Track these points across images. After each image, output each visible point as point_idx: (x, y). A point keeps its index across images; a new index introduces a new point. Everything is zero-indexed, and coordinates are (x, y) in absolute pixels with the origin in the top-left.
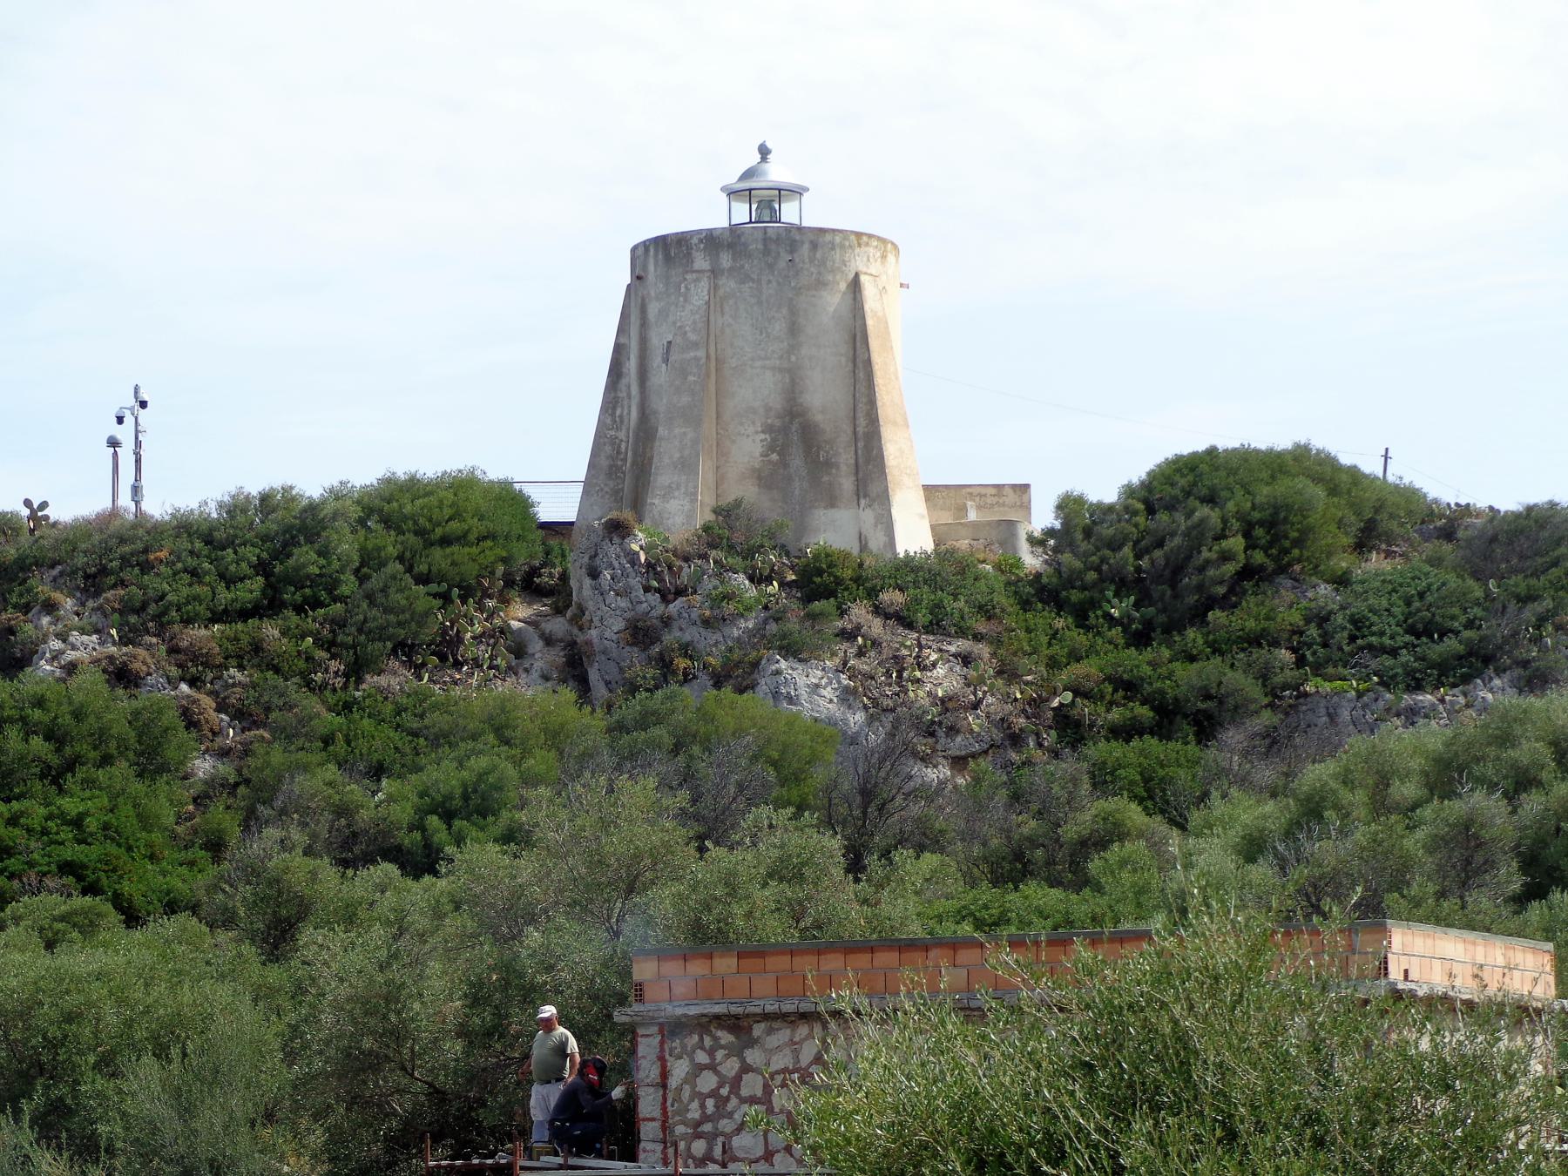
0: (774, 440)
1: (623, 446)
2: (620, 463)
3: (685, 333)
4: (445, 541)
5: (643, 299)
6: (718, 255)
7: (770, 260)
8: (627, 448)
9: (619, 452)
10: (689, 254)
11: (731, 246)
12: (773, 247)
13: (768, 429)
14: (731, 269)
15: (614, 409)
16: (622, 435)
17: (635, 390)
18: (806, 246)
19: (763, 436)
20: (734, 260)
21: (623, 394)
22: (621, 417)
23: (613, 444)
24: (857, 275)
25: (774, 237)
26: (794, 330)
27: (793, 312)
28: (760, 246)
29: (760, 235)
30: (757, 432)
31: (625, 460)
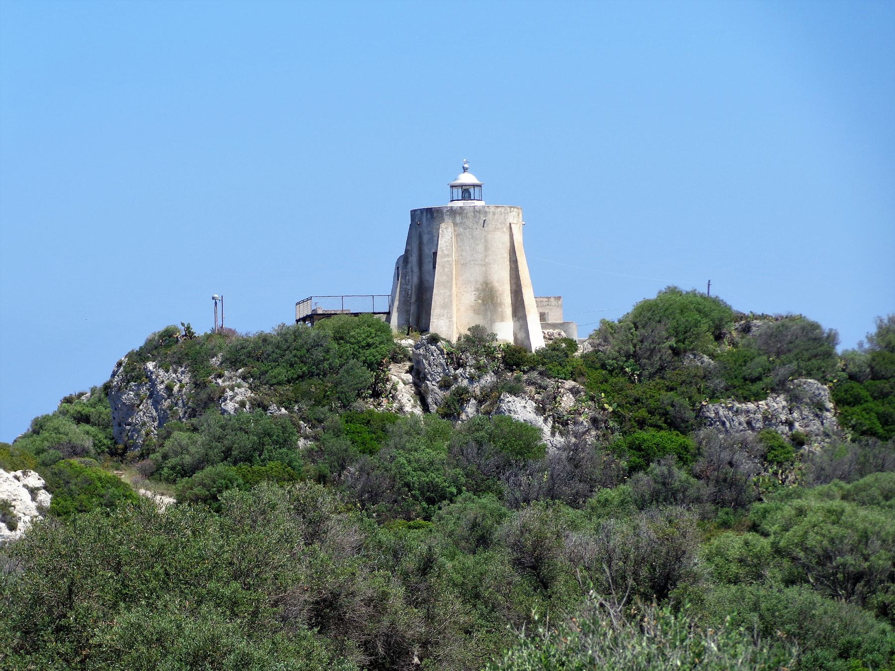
0: (479, 294)
1: (410, 291)
2: (408, 299)
3: (443, 250)
4: (369, 345)
5: (420, 233)
6: (455, 217)
7: (477, 220)
8: (411, 293)
9: (408, 295)
10: (442, 216)
11: (460, 214)
12: (478, 214)
13: (477, 290)
14: (461, 223)
15: (406, 276)
16: (409, 287)
17: (416, 269)
18: (491, 214)
19: (475, 293)
20: (462, 219)
21: (409, 270)
22: (408, 280)
23: (405, 291)
24: (510, 224)
25: (478, 210)
26: (486, 249)
27: (486, 241)
28: (472, 214)
29: (472, 209)
30: (472, 291)
31: (411, 298)
